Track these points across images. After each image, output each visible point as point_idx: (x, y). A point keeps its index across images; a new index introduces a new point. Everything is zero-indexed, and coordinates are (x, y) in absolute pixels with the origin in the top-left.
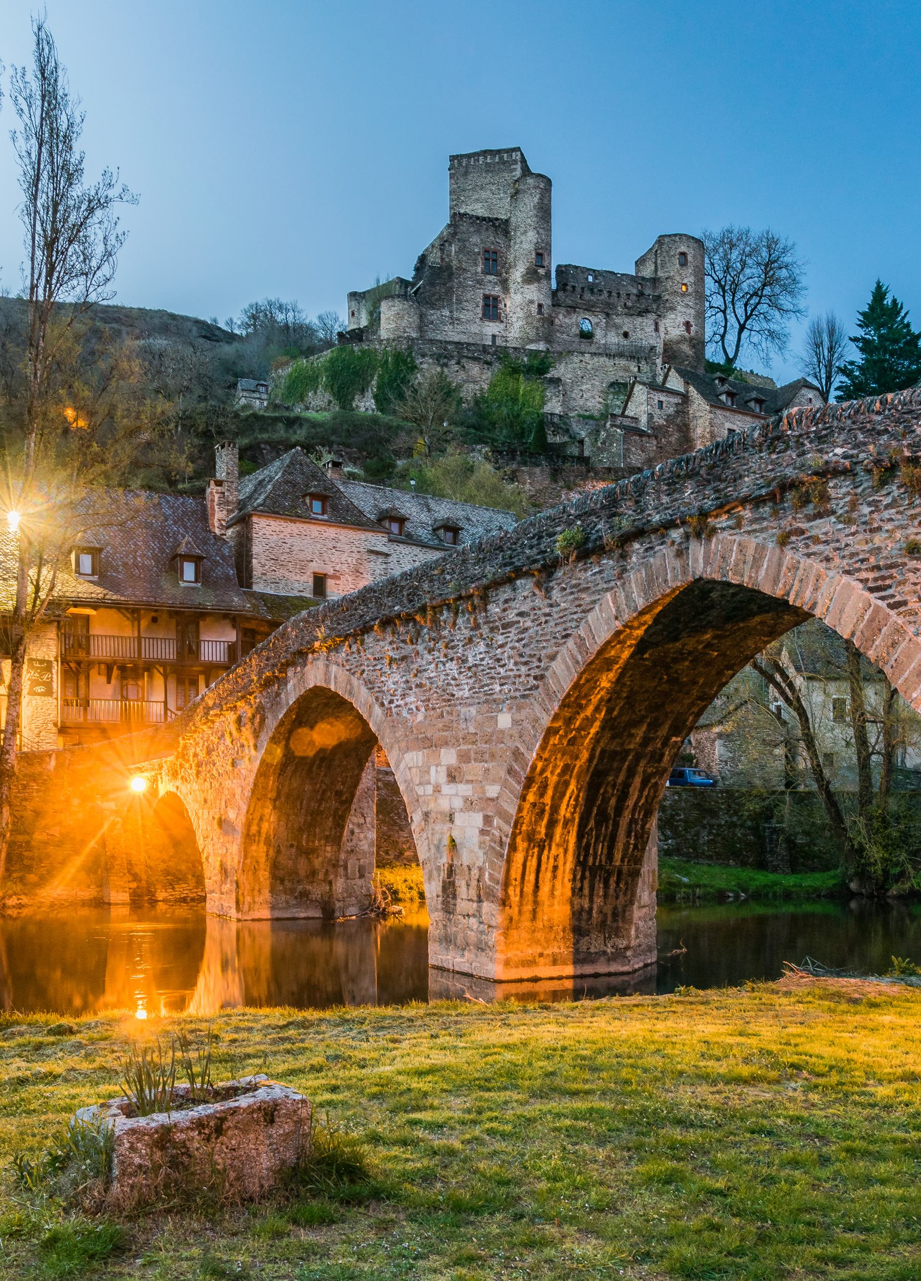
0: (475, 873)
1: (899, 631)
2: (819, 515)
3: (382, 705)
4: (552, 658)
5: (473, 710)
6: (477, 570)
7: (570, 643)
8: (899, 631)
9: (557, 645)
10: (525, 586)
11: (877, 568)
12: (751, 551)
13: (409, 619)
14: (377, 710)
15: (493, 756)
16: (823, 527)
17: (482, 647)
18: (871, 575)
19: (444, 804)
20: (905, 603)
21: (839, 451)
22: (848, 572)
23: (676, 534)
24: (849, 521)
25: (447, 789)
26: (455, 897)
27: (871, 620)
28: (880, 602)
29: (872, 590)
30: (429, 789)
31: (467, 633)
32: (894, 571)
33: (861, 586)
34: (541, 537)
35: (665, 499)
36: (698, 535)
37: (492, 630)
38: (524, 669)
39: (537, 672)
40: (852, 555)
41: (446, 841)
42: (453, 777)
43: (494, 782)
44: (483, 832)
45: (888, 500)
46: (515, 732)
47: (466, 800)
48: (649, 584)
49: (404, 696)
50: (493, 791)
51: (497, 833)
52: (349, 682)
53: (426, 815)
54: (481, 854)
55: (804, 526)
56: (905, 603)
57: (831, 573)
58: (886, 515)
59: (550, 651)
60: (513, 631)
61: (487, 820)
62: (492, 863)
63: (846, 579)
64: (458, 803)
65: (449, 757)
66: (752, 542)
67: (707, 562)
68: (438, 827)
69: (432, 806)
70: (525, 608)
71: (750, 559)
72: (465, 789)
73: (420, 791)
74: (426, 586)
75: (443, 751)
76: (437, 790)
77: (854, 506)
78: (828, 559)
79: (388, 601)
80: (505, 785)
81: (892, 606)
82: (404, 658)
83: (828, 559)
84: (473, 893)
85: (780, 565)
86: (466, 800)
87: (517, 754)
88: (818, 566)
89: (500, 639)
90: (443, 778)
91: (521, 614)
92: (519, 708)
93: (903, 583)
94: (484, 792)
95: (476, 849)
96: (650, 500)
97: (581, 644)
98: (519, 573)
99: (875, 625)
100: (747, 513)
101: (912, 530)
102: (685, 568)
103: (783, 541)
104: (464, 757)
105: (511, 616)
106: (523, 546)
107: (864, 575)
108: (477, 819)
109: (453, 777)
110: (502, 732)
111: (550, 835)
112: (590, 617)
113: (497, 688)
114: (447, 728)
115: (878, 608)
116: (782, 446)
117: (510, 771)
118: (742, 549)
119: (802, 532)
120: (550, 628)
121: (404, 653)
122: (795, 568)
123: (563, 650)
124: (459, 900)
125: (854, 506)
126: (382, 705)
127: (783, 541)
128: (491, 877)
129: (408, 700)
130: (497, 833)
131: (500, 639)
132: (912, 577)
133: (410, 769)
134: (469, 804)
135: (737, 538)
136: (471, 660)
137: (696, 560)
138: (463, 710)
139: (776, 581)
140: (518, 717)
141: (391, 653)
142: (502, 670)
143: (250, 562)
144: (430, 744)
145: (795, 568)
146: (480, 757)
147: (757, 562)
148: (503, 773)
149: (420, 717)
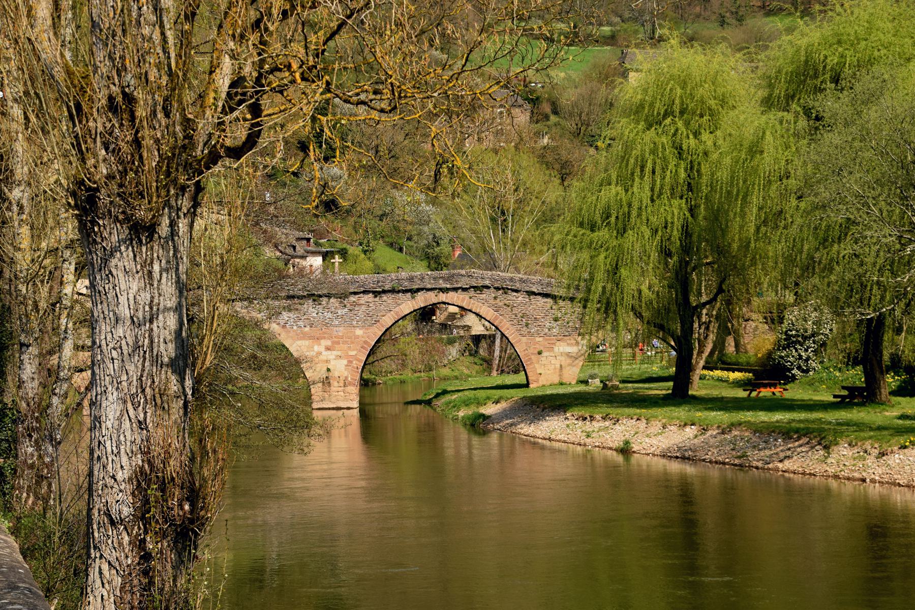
4: (383, 316)
7: (392, 312)
15: (353, 343)
19: (325, 358)
25: (325, 353)
34: (378, 282)
35: (432, 282)
38: (369, 318)
41: (325, 369)
43: (354, 350)
50: (353, 353)
51: (355, 366)
60: (363, 308)
65: (329, 343)
67: (446, 298)
70: (370, 300)
72: (335, 353)
80: (360, 351)
84: (342, 385)
88: (481, 304)
90: (322, 349)
94: (347, 353)
97: (397, 313)
99: (496, 318)
103: (470, 298)
104: (333, 343)
105: (362, 302)
106: (369, 283)
108: (345, 362)
114: (325, 333)
118: (458, 297)
120: (382, 308)
123: (389, 314)
124: (332, 388)
127: (470, 298)
128: (351, 379)
130: (355, 366)
133: (300, 347)
136: (340, 313)
146: (345, 343)
149: (307, 329)
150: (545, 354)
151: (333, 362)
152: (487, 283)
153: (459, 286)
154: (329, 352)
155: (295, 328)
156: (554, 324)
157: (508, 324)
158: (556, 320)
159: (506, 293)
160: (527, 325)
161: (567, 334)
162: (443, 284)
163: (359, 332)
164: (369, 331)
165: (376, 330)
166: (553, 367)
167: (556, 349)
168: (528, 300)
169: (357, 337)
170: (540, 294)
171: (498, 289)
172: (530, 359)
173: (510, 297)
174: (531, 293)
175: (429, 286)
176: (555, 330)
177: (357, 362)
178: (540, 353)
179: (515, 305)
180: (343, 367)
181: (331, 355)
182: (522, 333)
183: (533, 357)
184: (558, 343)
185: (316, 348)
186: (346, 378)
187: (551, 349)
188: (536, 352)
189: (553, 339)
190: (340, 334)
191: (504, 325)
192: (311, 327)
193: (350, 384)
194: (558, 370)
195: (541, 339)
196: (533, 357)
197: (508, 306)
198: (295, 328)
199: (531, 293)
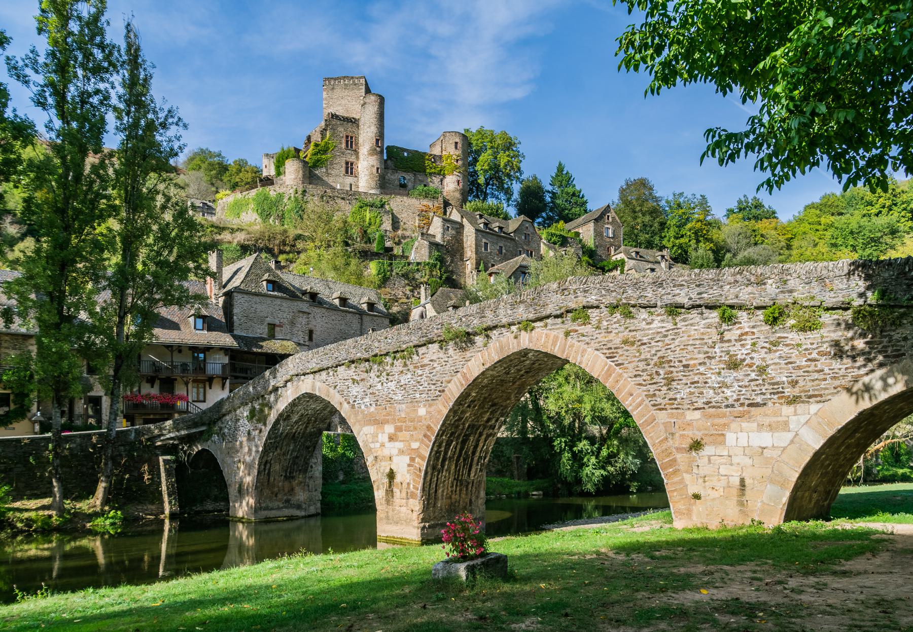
0: (405, 485)
1: (620, 375)
2: (584, 324)
3: (349, 403)
4: (449, 382)
5: (404, 406)
6: (407, 338)
7: (459, 375)
8: (620, 375)
9: (452, 376)
10: (436, 346)
11: (610, 348)
12: (552, 337)
13: (367, 360)
14: (346, 405)
15: (415, 429)
16: (587, 329)
17: (409, 376)
18: (607, 351)
19: (386, 452)
20: (623, 364)
21: (593, 297)
22: (597, 350)
23: (514, 328)
24: (598, 328)
25: (388, 445)
26: (393, 497)
27: (608, 370)
28: (613, 364)
29: (607, 358)
30: (378, 445)
31: (401, 369)
32: (619, 351)
33: (602, 356)
35: (509, 312)
36: (526, 329)
37: (415, 367)
38: (433, 387)
39: (441, 389)
40: (599, 342)
42: (391, 438)
43: (416, 441)
44: (409, 465)
45: (615, 320)
46: (428, 417)
47: (399, 450)
48: (502, 348)
49: (362, 399)
50: (415, 445)
52: (328, 391)
53: (376, 457)
54: (408, 476)
55: (577, 328)
56: (623, 364)
57: (589, 350)
58: (614, 326)
59: (447, 379)
60: (427, 369)
61: (412, 459)
62: (414, 480)
63: (596, 352)
64: (395, 452)
65: (389, 429)
66: (553, 333)
67: (530, 341)
68: (383, 463)
69: (379, 453)
70: (434, 358)
71: (551, 341)
72: (399, 445)
73: (372, 446)
74: (376, 344)
75: (386, 426)
76: (383, 445)
77: (600, 322)
78: (588, 343)
79: (354, 351)
80: (422, 442)
81: (617, 365)
82: (362, 380)
83: (588, 343)
85: (565, 345)
86: (399, 450)
87: (429, 428)
88: (583, 346)
89: (420, 372)
90: (386, 439)
91: (431, 361)
92: (430, 406)
93: (622, 355)
95: (406, 473)
96: (501, 312)
97: (464, 376)
98: (431, 342)
100: (549, 321)
101: (626, 333)
102: (519, 343)
103: (567, 334)
104: (399, 429)
105: (426, 361)
107: (605, 351)
108: (407, 459)
109: (391, 438)
110: (421, 417)
111: (443, 466)
112: (469, 363)
113: (418, 396)
114: (388, 414)
115: (610, 366)
116: (566, 293)
117: (425, 436)
119: (576, 331)
120: (447, 368)
121: (362, 377)
122: (572, 346)
123: (455, 379)
125: (600, 322)
126: (349, 403)
127: (567, 334)
128: (415, 487)
129: (365, 400)
131: (420, 372)
132: (626, 354)
134: (401, 452)
135: (545, 332)
137: (524, 340)
138: (398, 406)
139: (563, 352)
140: (429, 410)
141: (355, 377)
142: (421, 388)
143: (232, 318)
144: (379, 423)
145: (572, 346)
147: (554, 344)
148: (421, 436)
149: (372, 409)
150: (708, 450)
151: (395, 459)
152: (592, 299)
153: (548, 312)
154: (392, 444)
155: (363, 407)
156: (731, 376)
157: (632, 383)
158: (734, 365)
159: (628, 315)
160: (670, 381)
161: (759, 399)
162: (522, 313)
163: (422, 411)
164: (432, 409)
165: (441, 407)
166: (723, 482)
167: (730, 437)
168: (670, 326)
169: (420, 419)
170: (694, 307)
171: (614, 308)
172: (675, 460)
173: (633, 323)
174: (674, 309)
175: (505, 321)
176: (728, 393)
177: (420, 461)
178: (696, 446)
179: (645, 340)
180: (406, 468)
181: (392, 448)
182: (659, 400)
183: (679, 456)
184: (733, 426)
185: (380, 435)
186: (408, 484)
187: (719, 440)
188: (686, 444)
189: (724, 416)
190: (403, 416)
191: (625, 386)
192: (376, 405)
193: (413, 496)
194: (735, 492)
195: (697, 415)
196: (679, 456)
197: (633, 344)
198: (363, 407)
199: (674, 309)
